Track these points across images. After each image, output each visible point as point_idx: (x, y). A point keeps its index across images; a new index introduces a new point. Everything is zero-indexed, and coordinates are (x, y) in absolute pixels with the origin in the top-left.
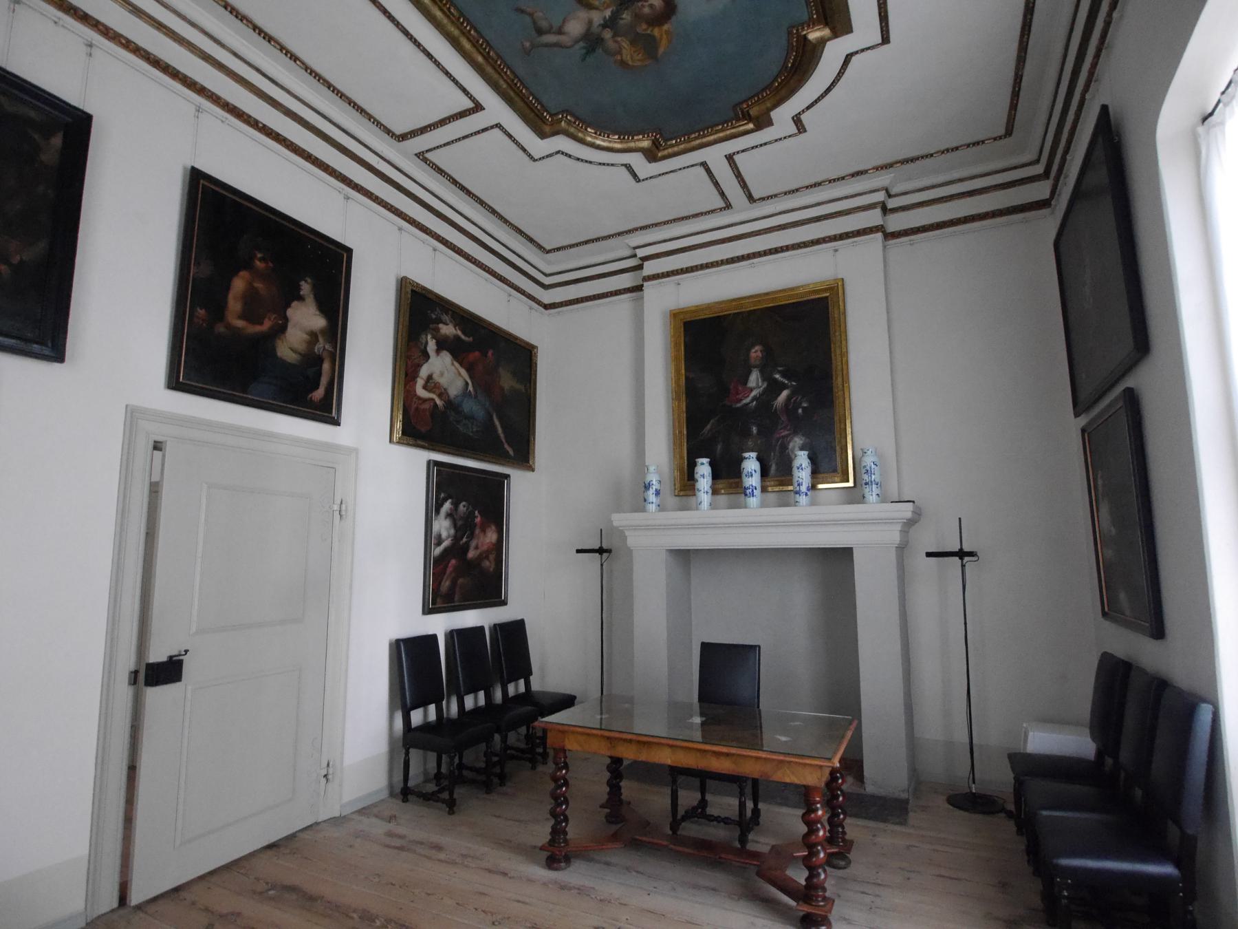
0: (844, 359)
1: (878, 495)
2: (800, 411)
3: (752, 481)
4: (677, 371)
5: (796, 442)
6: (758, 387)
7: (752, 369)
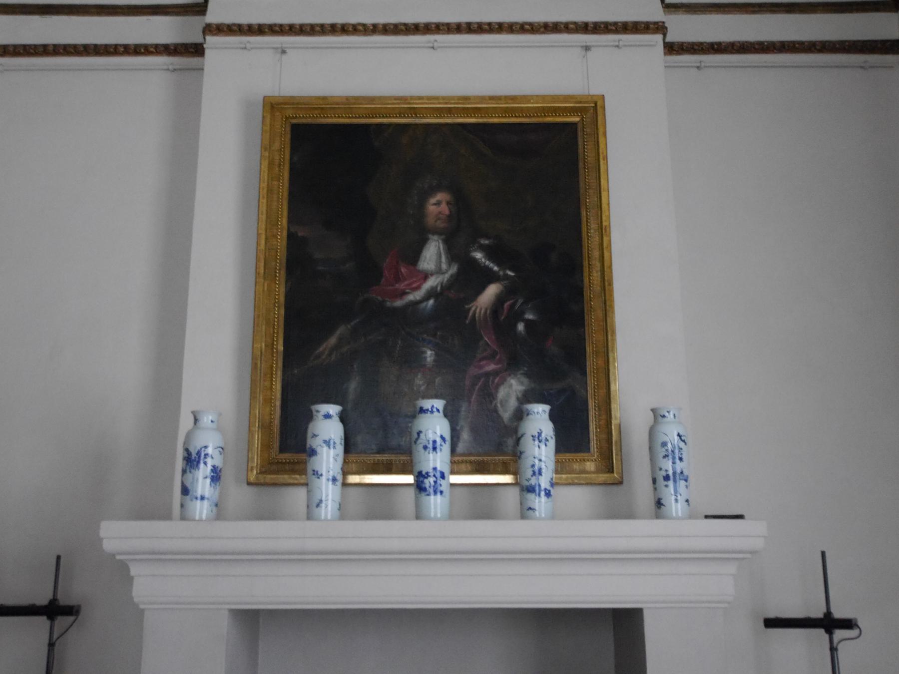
0: (605, 239)
1: (687, 501)
2: (521, 327)
3: (435, 460)
4: (271, 222)
5: (511, 386)
6: (439, 271)
7: (430, 236)
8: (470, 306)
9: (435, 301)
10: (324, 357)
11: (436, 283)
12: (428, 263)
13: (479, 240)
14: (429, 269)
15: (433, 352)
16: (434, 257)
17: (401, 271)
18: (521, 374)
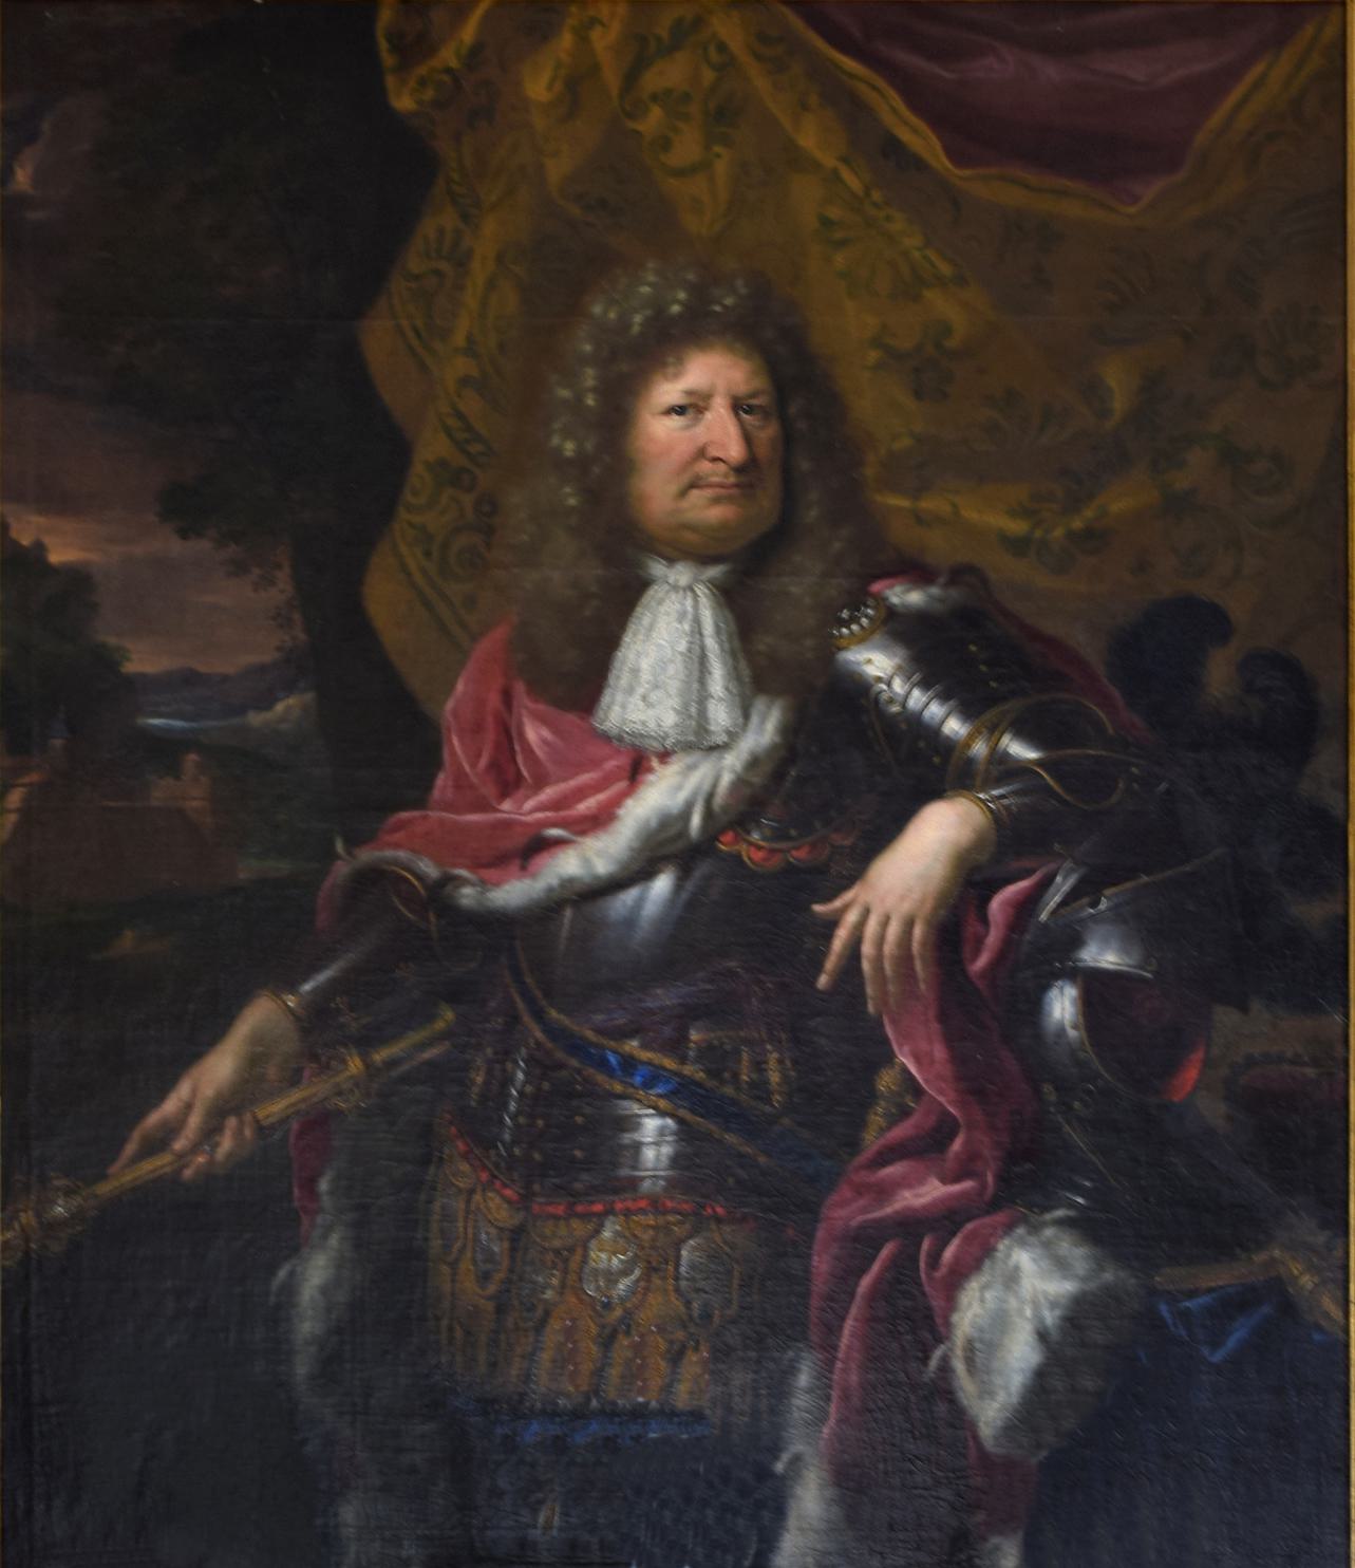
2: (1063, 1006)
5: (1012, 1279)
6: (699, 741)
7: (658, 568)
8: (838, 903)
9: (678, 887)
10: (179, 1145)
11: (682, 797)
12: (644, 698)
13: (876, 587)
14: (652, 725)
15: (669, 1122)
18: (1059, 1222)
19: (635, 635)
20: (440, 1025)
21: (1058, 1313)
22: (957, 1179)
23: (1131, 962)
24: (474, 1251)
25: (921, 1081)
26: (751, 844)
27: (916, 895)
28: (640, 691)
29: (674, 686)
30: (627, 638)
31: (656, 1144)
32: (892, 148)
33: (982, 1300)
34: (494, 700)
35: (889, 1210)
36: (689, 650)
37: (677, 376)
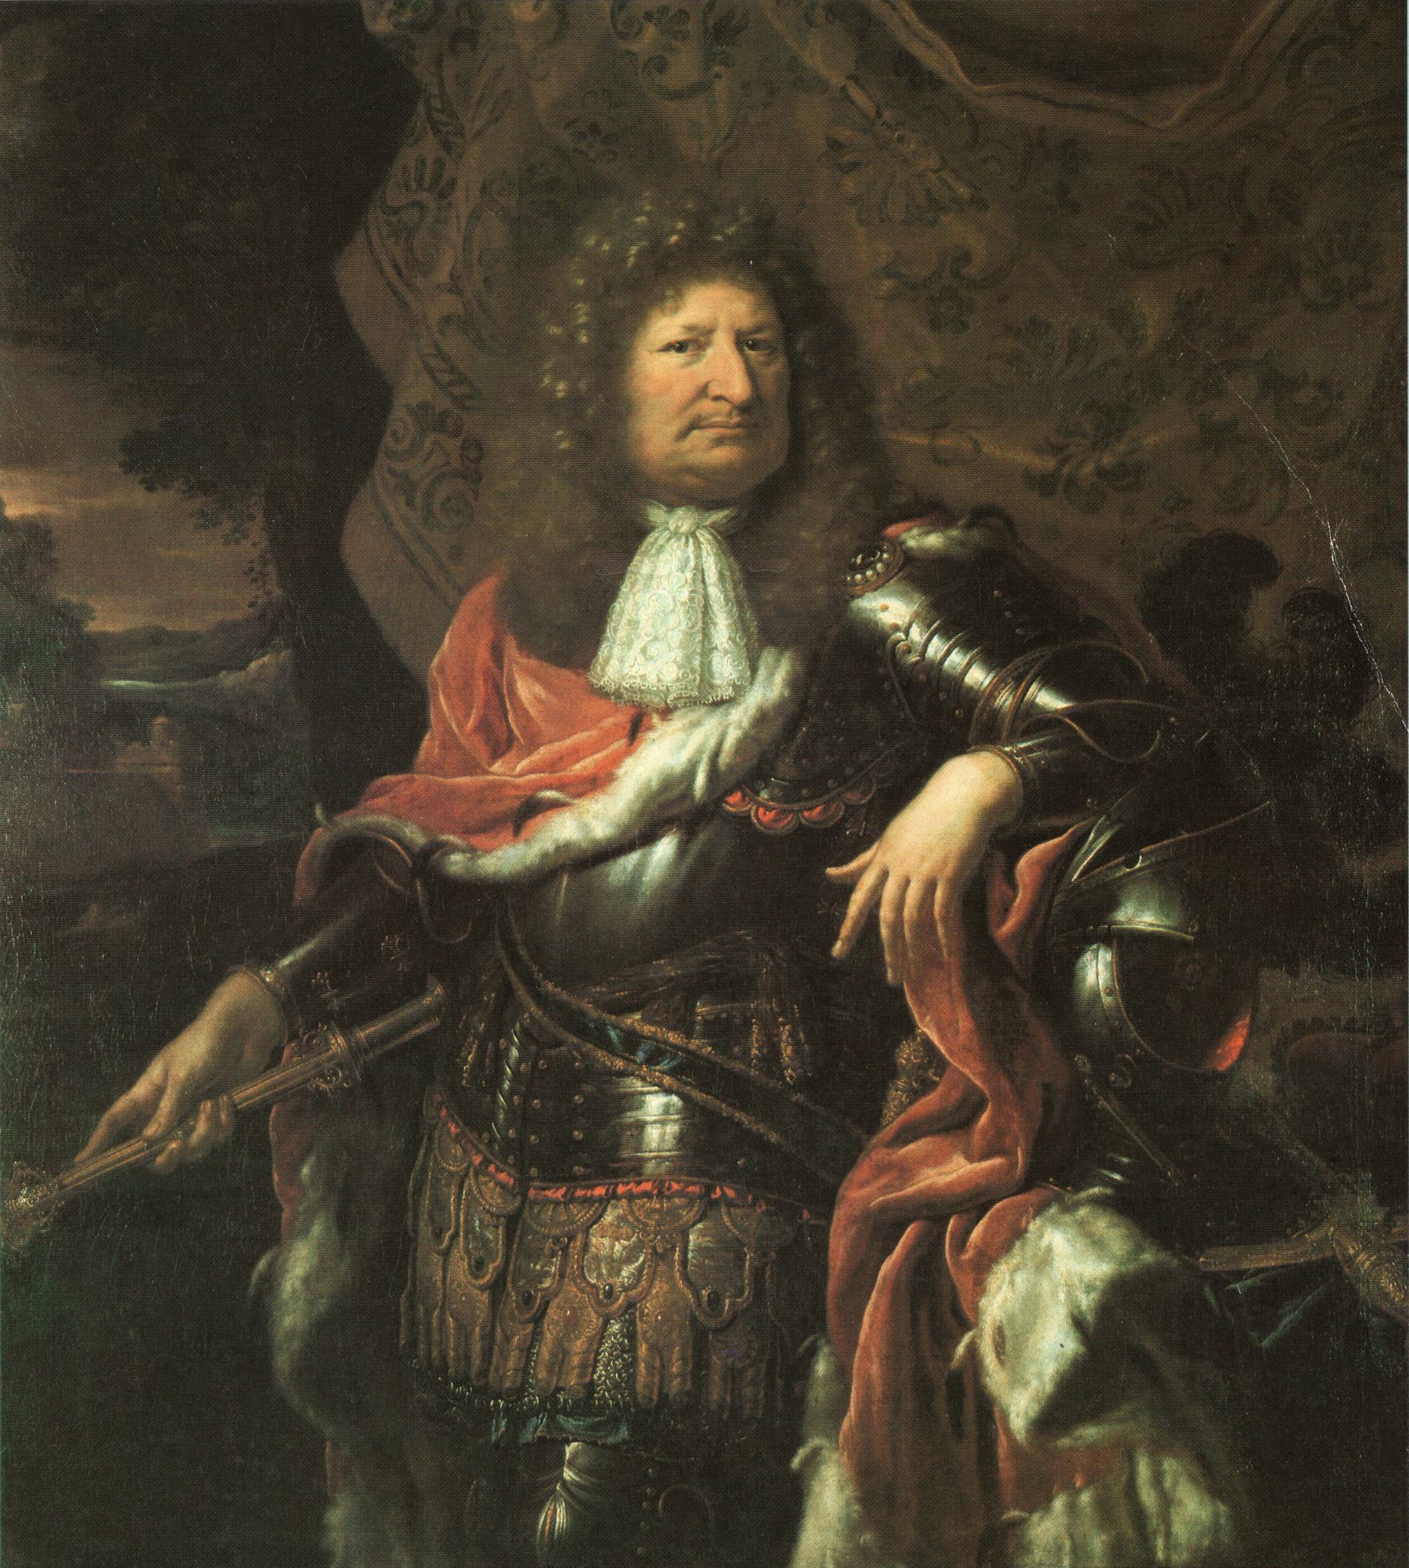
5: (1044, 1262)
7: (656, 514)
8: (853, 865)
9: (682, 851)
10: (151, 1130)
13: (891, 530)
14: (652, 679)
15: (674, 1099)
16: (677, 624)
17: (513, 692)
18: (1097, 1202)
19: (633, 585)
20: (427, 1001)
21: (1093, 1295)
22: (983, 1157)
23: (1168, 923)
24: (466, 1238)
25: (943, 1051)
26: (759, 805)
27: (936, 856)
28: (638, 645)
29: (676, 637)
30: (625, 588)
31: (663, 1123)
32: (906, 66)
33: (1012, 1283)
34: (483, 654)
35: (910, 1190)
36: (692, 600)
37: (675, 310)
